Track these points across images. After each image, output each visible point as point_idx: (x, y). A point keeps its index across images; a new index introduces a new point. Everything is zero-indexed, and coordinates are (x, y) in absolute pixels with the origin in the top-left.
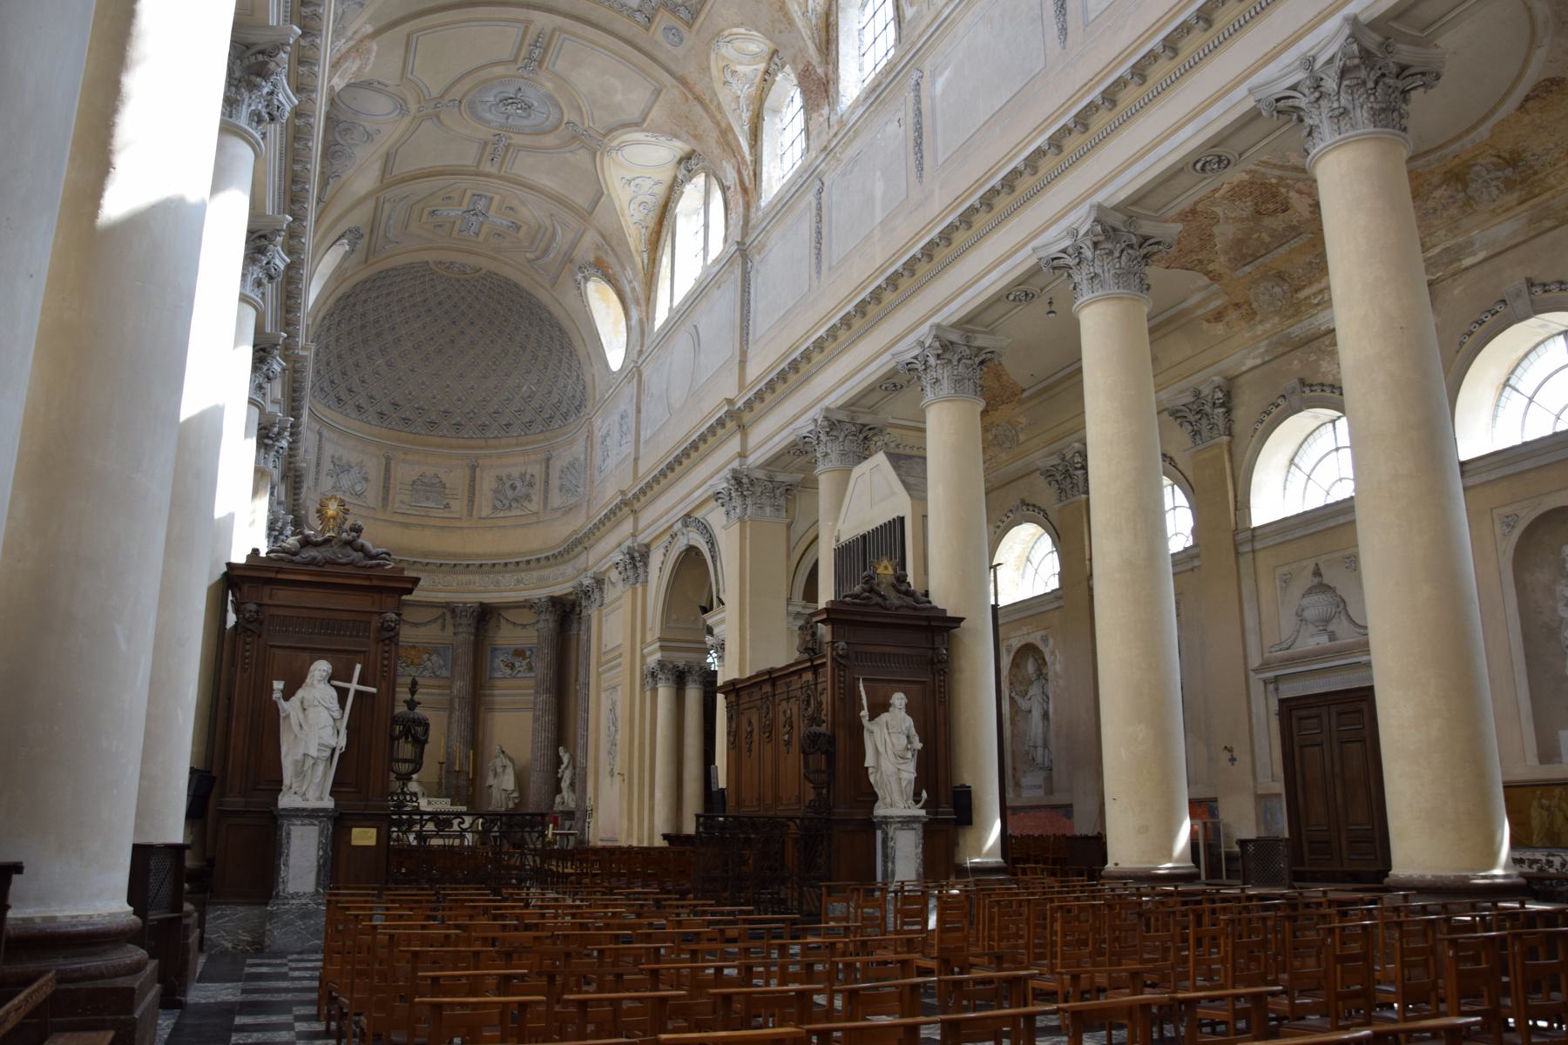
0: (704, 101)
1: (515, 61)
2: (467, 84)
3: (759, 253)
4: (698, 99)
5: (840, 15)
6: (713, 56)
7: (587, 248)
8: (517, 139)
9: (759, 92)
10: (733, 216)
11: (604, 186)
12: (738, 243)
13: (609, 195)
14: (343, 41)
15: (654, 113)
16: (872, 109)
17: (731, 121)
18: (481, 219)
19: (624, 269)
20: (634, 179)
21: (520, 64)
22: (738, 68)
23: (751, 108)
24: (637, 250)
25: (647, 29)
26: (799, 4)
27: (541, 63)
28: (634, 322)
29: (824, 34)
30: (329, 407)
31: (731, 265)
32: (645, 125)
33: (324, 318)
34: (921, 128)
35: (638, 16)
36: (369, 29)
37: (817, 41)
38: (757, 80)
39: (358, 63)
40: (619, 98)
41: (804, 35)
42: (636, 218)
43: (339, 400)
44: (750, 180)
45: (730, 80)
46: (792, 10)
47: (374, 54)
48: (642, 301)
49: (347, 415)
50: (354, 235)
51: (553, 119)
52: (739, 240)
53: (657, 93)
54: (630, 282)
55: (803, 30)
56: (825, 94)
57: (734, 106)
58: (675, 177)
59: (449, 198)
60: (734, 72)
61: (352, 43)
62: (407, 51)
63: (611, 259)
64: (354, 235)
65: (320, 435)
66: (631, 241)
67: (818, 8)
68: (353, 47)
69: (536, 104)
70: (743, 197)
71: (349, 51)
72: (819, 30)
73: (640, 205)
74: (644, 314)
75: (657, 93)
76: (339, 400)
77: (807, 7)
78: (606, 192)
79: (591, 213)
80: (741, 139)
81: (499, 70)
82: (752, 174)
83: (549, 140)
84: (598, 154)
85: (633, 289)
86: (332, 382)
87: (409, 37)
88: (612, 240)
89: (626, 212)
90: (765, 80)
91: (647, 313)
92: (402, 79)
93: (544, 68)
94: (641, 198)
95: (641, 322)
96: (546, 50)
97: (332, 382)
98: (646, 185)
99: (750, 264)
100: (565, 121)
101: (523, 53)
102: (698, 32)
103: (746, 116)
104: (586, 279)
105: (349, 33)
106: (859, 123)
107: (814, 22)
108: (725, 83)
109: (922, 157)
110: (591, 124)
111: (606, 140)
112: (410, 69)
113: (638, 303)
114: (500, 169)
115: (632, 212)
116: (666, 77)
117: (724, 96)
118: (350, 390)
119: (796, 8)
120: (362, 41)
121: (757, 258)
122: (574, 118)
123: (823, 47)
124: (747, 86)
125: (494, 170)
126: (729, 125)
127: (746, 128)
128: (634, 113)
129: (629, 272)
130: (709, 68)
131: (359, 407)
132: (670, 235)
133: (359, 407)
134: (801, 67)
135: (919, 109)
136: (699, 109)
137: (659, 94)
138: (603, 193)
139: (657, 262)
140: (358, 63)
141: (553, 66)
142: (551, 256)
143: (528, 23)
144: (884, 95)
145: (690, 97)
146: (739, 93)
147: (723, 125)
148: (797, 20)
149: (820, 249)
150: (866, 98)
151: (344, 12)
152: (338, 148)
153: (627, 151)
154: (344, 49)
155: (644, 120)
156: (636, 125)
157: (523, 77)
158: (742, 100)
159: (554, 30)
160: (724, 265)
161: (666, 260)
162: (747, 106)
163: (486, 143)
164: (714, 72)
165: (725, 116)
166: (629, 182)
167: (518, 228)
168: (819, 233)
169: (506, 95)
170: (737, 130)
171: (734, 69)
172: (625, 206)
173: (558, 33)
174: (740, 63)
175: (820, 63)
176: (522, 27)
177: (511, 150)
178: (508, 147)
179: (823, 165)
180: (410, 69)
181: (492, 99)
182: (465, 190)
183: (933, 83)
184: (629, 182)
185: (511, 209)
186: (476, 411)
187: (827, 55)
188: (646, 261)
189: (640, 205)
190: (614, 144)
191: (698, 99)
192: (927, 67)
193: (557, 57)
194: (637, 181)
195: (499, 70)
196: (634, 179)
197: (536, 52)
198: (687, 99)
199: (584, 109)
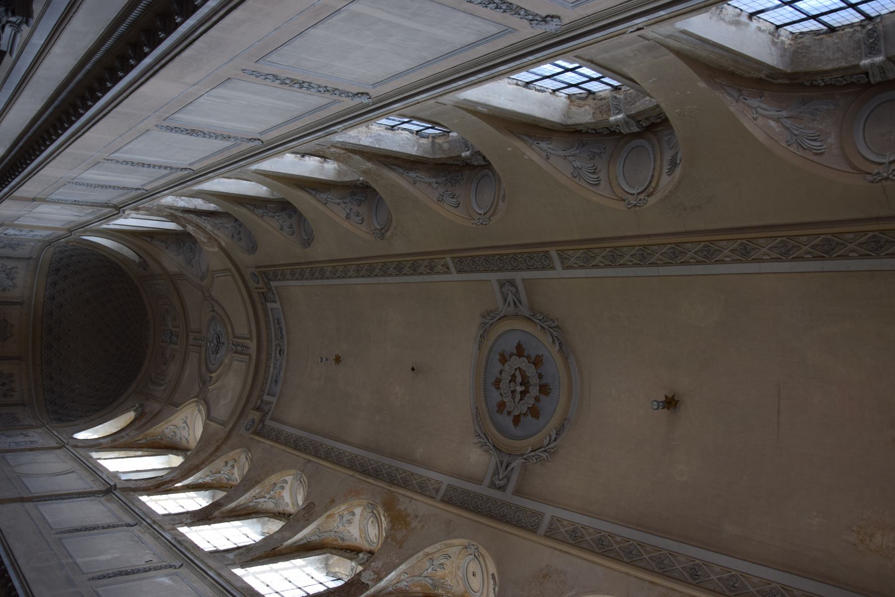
0: (217, 452)
1: (235, 337)
2: (221, 312)
3: (106, 500)
4: (218, 448)
5: (255, 519)
6: (239, 450)
7: (154, 406)
8: (203, 349)
9: (225, 485)
10: (144, 482)
11: (183, 406)
12: (115, 485)
13: (177, 411)
14: (211, 228)
15: (212, 423)
16: (169, 544)
17: (202, 471)
18: (169, 341)
19: (136, 430)
20: (187, 425)
21: (235, 340)
22: (236, 468)
23: (214, 482)
24: (146, 435)
25: (253, 409)
26: (260, 492)
27: (236, 352)
28: (102, 441)
29: (245, 512)
30: (51, 264)
31: (104, 485)
32: (207, 421)
33: (104, 256)
34: (134, 573)
35: (259, 402)
36: (223, 244)
37: (238, 508)
38: (231, 482)
39: (206, 241)
40: (222, 403)
41: (241, 499)
42: (166, 431)
43: (58, 270)
44: (165, 488)
45: (228, 465)
46: (255, 488)
47: (214, 250)
48: (115, 444)
49: (48, 276)
50: (144, 264)
51: (211, 367)
52: (118, 486)
53: (223, 424)
54: (127, 435)
55: (243, 498)
56: (200, 519)
57: (214, 470)
58: (188, 450)
59: (175, 319)
60: (233, 466)
61: (213, 235)
62: (222, 270)
63: (143, 421)
64: (144, 264)
65: (30, 258)
66: (152, 430)
67: (260, 506)
68: (212, 236)
69: (218, 356)
70: (153, 486)
71: (207, 233)
72: (246, 508)
73: (173, 432)
74: (106, 446)
75: (223, 424)
76: (58, 270)
77: (260, 498)
78: (178, 409)
79: (170, 404)
80: (192, 478)
81: (230, 330)
82: (168, 488)
83: (204, 369)
84: (196, 399)
85: (123, 437)
86: (69, 265)
87: (229, 269)
88: (156, 418)
89: (169, 424)
90: (231, 487)
91: (105, 448)
92: (212, 271)
93: (234, 355)
94: (178, 432)
95: (100, 444)
96: (241, 353)
97: (69, 265)
98: (185, 433)
99: (100, 495)
100: (212, 375)
101: (239, 341)
102: (252, 438)
103: (208, 479)
104: (135, 411)
105: (216, 232)
106: (162, 538)
107: (250, 504)
108: (226, 463)
109: (110, 577)
110: (210, 390)
111: (202, 401)
112: (218, 275)
113: (112, 441)
114: (192, 345)
115: (170, 428)
116: (230, 426)
117: (219, 463)
118: (66, 277)
119: (257, 491)
120: (216, 241)
121: (103, 499)
122: (214, 380)
123: (234, 514)
124: (226, 476)
125: (191, 342)
126: (201, 469)
127: (201, 481)
128: (215, 414)
129: (134, 433)
130: (233, 450)
131: (55, 284)
132: (155, 453)
133: (55, 284)
134: (222, 502)
135: (150, 570)
136: (212, 449)
137: (222, 425)
138: (177, 407)
139: (141, 449)
140: (206, 241)
141: (235, 360)
142: (151, 387)
143: (250, 339)
144: (174, 549)
145: (218, 444)
146: (222, 472)
147: (202, 466)
148: (249, 493)
149: (81, 530)
150: (179, 542)
151: (228, 228)
152: (182, 245)
153: (199, 415)
154: (207, 229)
155: (210, 420)
156: (209, 417)
157: (228, 344)
158: (218, 475)
159: (250, 355)
160: (105, 480)
161: (139, 453)
162: (215, 480)
163: (199, 333)
164: (231, 454)
165: (206, 466)
166: (185, 422)
167: (165, 365)
168: (94, 529)
169: (221, 337)
170: (198, 475)
171: (235, 466)
172: (173, 423)
173: (248, 357)
174: (238, 469)
175: (222, 513)
176: (248, 336)
177: (199, 348)
178: (201, 346)
179: (145, 524)
180: (218, 275)
181: (218, 330)
182: (179, 327)
183: (166, 575)
184: (185, 422)
185: (174, 357)
186: (61, 357)
187: (229, 517)
188: (140, 442)
189: (173, 432)
190: (201, 407)
191: (218, 448)
192: (184, 571)
193: (239, 361)
194: (186, 427)
195: (230, 330)
196: (187, 425)
197: (242, 350)
198: (217, 442)
199: (217, 384)
